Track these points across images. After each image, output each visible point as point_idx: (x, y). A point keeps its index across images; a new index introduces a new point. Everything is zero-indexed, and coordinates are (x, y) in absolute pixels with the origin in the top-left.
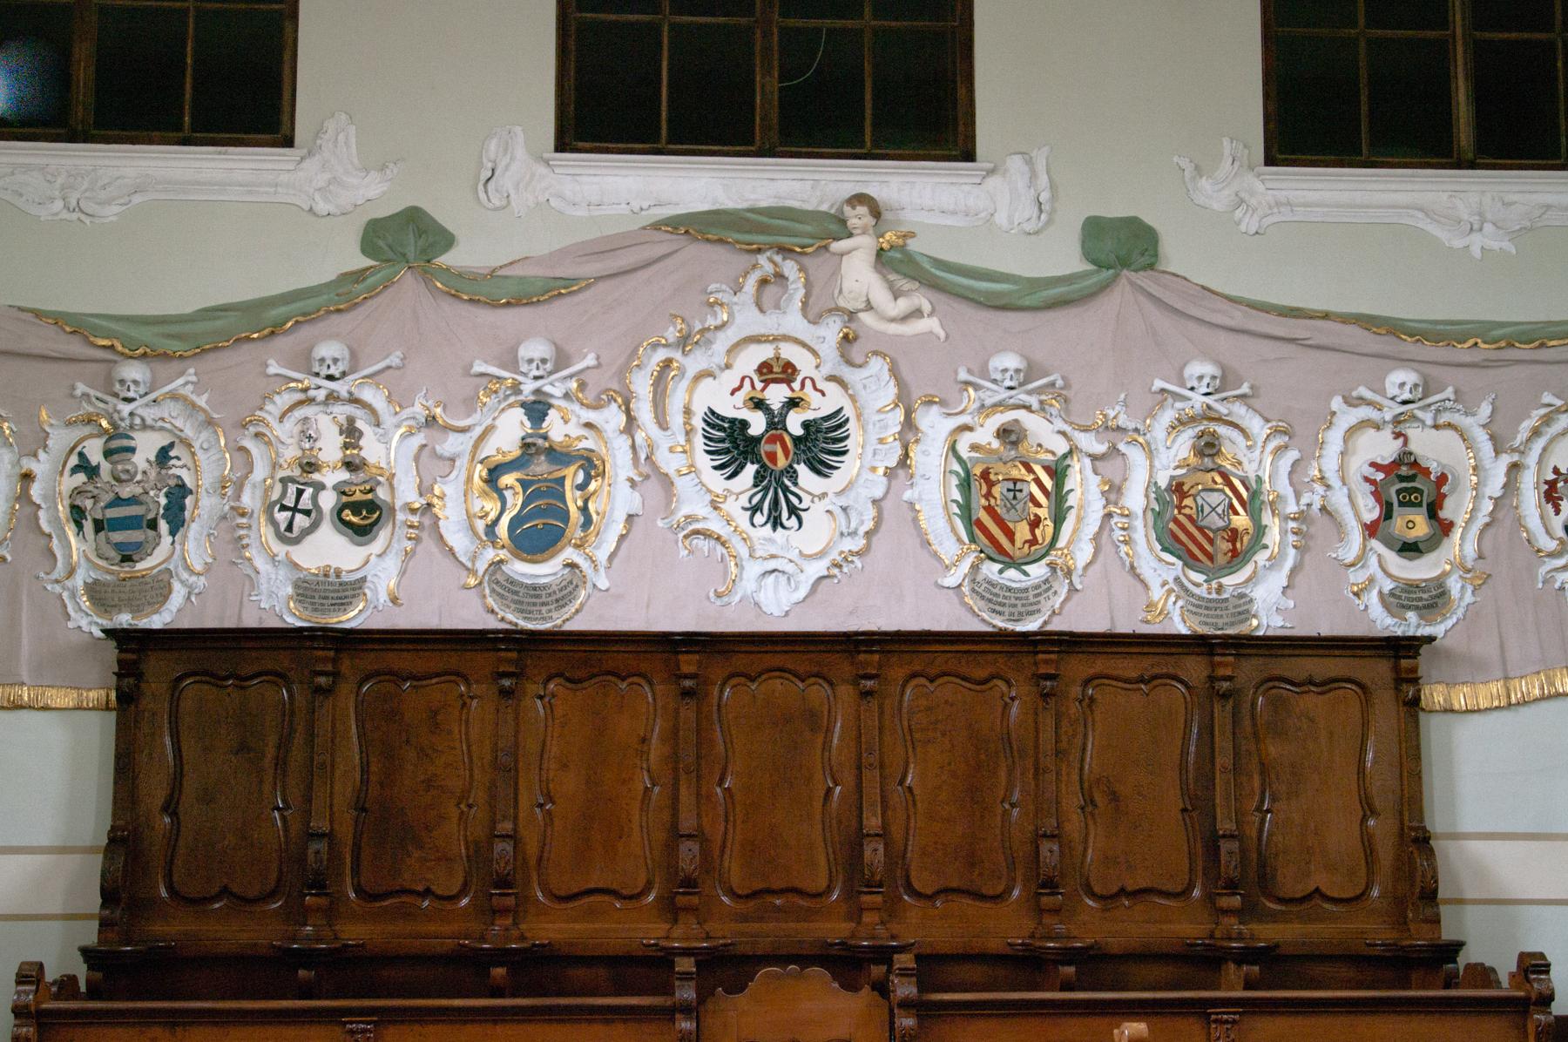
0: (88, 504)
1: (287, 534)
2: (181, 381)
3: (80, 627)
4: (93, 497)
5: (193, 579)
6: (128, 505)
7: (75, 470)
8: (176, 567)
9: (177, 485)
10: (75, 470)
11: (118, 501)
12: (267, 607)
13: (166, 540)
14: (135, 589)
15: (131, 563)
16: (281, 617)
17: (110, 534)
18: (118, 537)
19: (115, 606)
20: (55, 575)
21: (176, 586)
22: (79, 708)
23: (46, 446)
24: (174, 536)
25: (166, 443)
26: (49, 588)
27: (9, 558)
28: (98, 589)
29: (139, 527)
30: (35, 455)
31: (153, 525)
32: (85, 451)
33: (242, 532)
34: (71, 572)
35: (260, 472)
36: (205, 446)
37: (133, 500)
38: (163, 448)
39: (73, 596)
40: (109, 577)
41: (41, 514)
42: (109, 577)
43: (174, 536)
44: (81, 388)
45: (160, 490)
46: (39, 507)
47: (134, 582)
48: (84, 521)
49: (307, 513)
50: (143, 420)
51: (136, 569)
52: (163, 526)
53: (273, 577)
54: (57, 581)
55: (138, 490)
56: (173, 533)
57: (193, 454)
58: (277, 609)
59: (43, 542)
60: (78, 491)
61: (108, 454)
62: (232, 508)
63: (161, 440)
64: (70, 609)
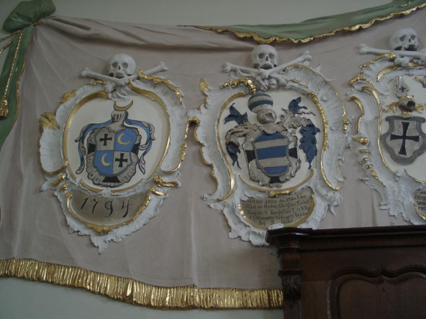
0: (240, 141)
1: (402, 156)
2: (301, 59)
3: (239, 237)
4: (244, 135)
5: (330, 194)
6: (273, 139)
7: (227, 119)
8: (316, 185)
9: (308, 125)
10: (227, 119)
11: (265, 136)
12: (396, 214)
13: (305, 165)
14: (284, 204)
15: (278, 184)
16: (409, 221)
17: (260, 161)
18: (268, 163)
19: (268, 218)
20: (217, 196)
21: (317, 200)
22: (244, 308)
23: (205, 103)
24: (310, 162)
25: (295, 98)
26: (212, 206)
27: (180, 184)
28: (253, 205)
29: (284, 155)
30: (199, 109)
31: (293, 153)
32: (234, 106)
33: (365, 156)
34: (229, 193)
35: (369, 116)
36: (325, 98)
37: (277, 135)
38: (294, 101)
39: (233, 211)
40: (261, 195)
41: (204, 150)
42: (261, 195)
43: (310, 162)
44: (229, 66)
45: (296, 128)
46: (202, 145)
47: (282, 198)
48: (238, 154)
49: (416, 139)
50: (278, 81)
51: (282, 188)
52: (301, 154)
53: (397, 189)
54: (218, 201)
55: (279, 129)
56: (309, 159)
57: (315, 103)
58: (404, 215)
59: (206, 171)
60: (232, 133)
61: (251, 106)
62: (354, 140)
63: (291, 96)
64: (231, 223)
